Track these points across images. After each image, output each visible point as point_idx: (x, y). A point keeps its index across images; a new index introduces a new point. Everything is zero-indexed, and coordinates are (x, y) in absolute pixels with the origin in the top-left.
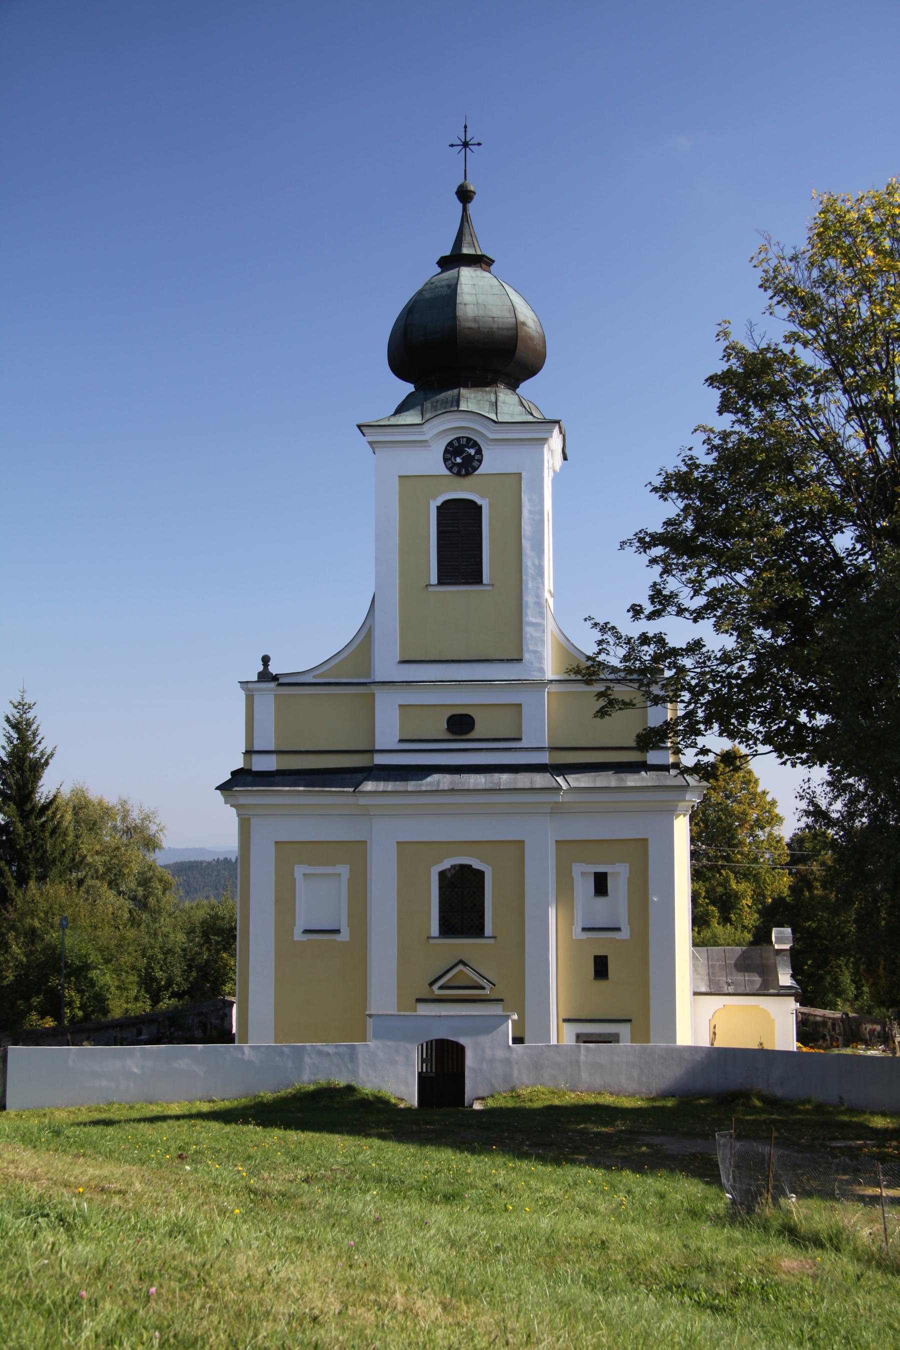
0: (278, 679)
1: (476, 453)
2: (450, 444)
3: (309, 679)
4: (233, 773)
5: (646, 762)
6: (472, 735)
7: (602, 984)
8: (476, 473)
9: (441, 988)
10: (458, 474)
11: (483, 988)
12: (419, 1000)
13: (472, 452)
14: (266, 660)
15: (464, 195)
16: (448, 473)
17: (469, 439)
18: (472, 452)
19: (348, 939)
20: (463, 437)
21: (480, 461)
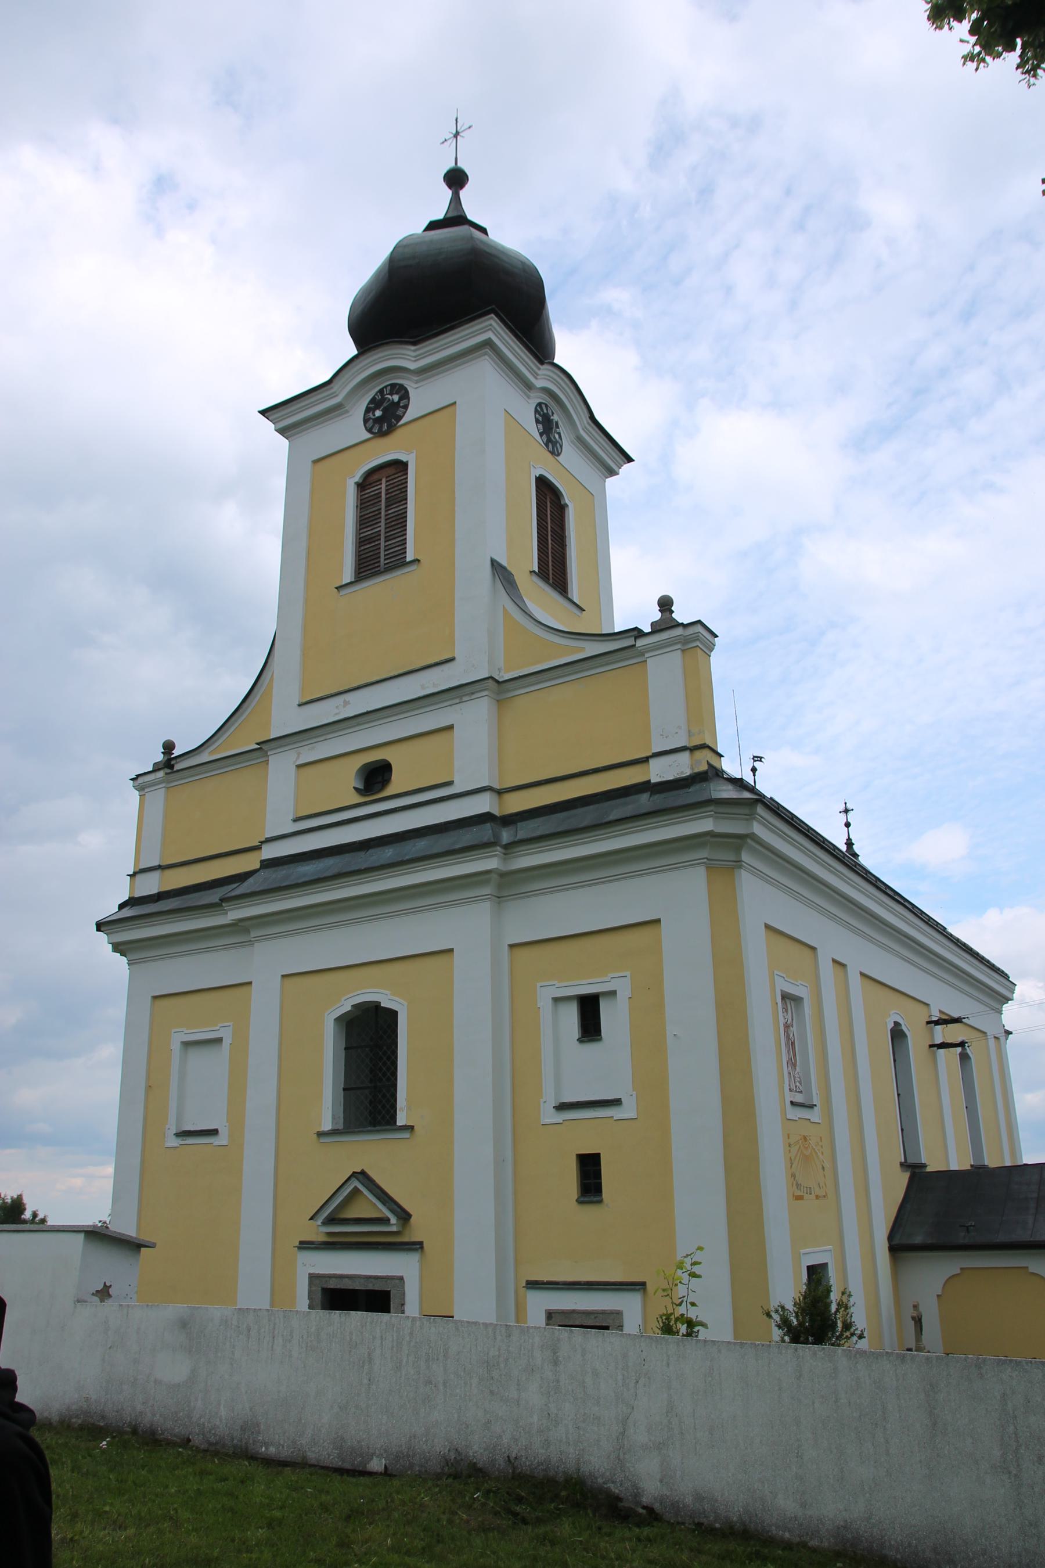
0: (172, 767)
1: (400, 399)
2: (373, 400)
3: (205, 757)
4: (121, 906)
5: (649, 781)
6: (389, 791)
7: (590, 1211)
8: (402, 422)
9: (331, 1220)
10: (382, 434)
11: (385, 1221)
12: (305, 1245)
13: (396, 398)
14: (169, 747)
15: (456, 179)
16: (369, 436)
17: (393, 386)
18: (396, 398)
19: (225, 1143)
20: (386, 387)
21: (406, 407)
